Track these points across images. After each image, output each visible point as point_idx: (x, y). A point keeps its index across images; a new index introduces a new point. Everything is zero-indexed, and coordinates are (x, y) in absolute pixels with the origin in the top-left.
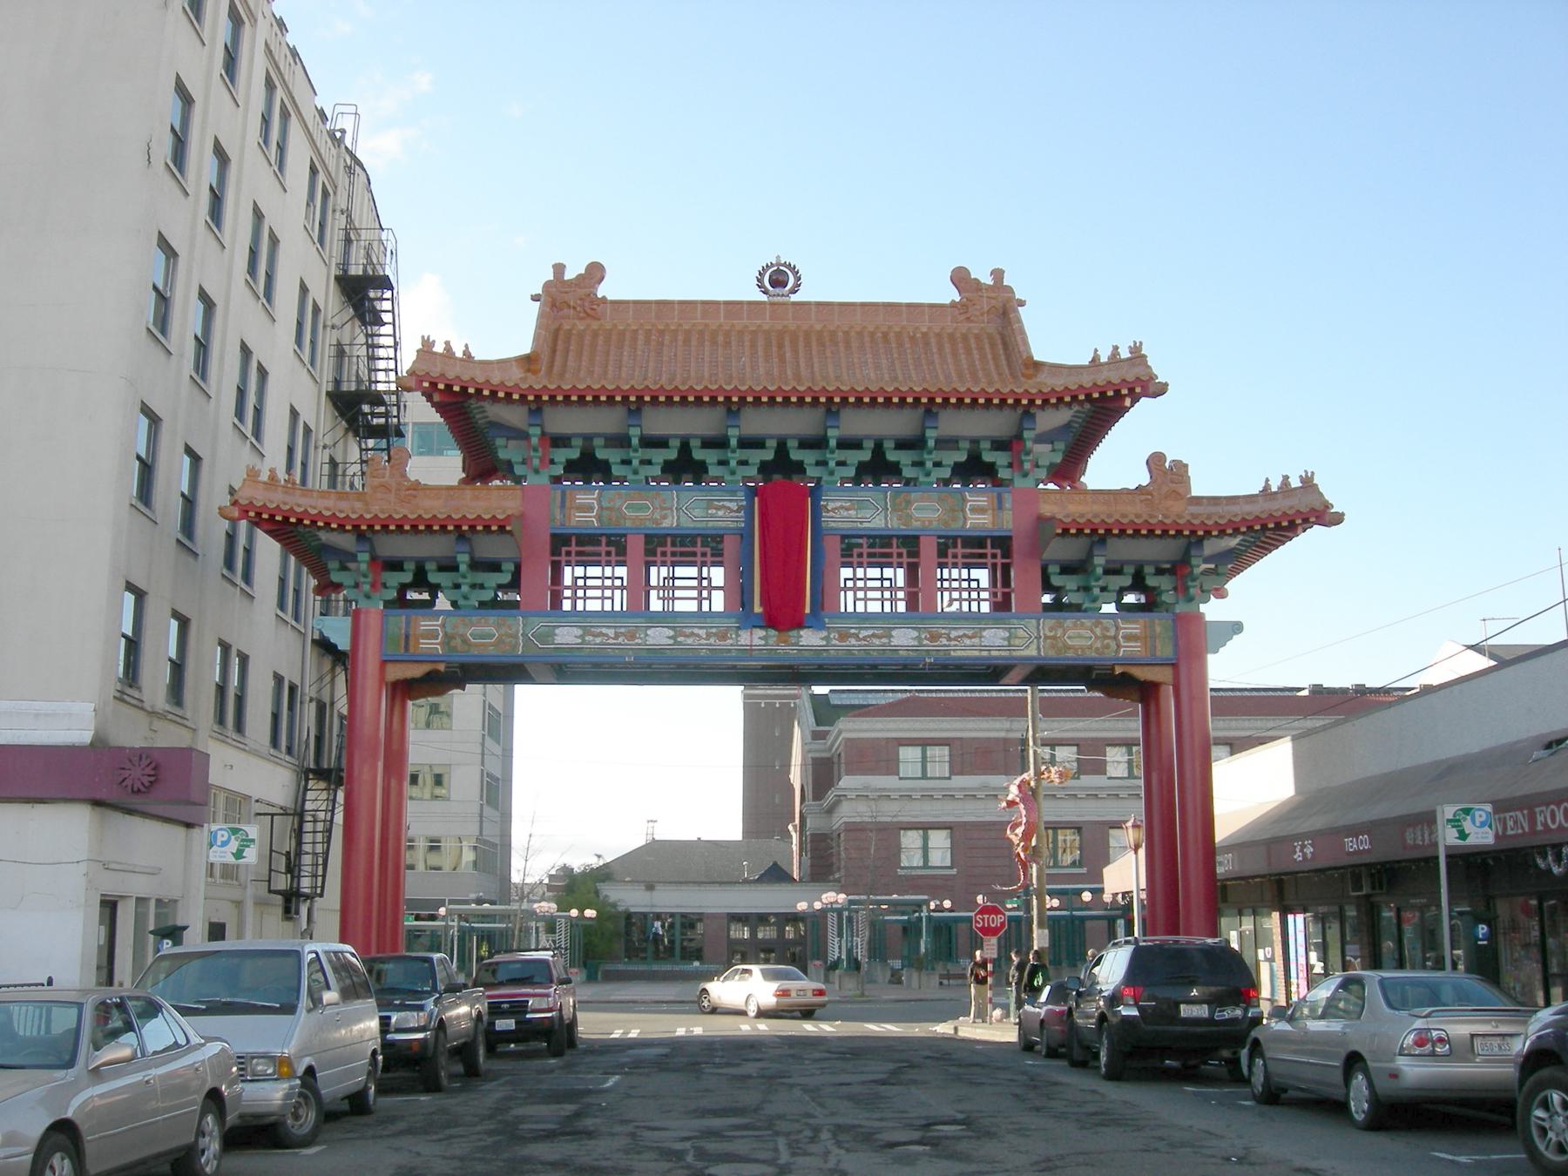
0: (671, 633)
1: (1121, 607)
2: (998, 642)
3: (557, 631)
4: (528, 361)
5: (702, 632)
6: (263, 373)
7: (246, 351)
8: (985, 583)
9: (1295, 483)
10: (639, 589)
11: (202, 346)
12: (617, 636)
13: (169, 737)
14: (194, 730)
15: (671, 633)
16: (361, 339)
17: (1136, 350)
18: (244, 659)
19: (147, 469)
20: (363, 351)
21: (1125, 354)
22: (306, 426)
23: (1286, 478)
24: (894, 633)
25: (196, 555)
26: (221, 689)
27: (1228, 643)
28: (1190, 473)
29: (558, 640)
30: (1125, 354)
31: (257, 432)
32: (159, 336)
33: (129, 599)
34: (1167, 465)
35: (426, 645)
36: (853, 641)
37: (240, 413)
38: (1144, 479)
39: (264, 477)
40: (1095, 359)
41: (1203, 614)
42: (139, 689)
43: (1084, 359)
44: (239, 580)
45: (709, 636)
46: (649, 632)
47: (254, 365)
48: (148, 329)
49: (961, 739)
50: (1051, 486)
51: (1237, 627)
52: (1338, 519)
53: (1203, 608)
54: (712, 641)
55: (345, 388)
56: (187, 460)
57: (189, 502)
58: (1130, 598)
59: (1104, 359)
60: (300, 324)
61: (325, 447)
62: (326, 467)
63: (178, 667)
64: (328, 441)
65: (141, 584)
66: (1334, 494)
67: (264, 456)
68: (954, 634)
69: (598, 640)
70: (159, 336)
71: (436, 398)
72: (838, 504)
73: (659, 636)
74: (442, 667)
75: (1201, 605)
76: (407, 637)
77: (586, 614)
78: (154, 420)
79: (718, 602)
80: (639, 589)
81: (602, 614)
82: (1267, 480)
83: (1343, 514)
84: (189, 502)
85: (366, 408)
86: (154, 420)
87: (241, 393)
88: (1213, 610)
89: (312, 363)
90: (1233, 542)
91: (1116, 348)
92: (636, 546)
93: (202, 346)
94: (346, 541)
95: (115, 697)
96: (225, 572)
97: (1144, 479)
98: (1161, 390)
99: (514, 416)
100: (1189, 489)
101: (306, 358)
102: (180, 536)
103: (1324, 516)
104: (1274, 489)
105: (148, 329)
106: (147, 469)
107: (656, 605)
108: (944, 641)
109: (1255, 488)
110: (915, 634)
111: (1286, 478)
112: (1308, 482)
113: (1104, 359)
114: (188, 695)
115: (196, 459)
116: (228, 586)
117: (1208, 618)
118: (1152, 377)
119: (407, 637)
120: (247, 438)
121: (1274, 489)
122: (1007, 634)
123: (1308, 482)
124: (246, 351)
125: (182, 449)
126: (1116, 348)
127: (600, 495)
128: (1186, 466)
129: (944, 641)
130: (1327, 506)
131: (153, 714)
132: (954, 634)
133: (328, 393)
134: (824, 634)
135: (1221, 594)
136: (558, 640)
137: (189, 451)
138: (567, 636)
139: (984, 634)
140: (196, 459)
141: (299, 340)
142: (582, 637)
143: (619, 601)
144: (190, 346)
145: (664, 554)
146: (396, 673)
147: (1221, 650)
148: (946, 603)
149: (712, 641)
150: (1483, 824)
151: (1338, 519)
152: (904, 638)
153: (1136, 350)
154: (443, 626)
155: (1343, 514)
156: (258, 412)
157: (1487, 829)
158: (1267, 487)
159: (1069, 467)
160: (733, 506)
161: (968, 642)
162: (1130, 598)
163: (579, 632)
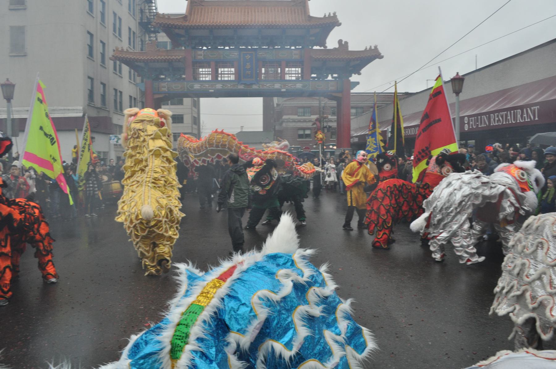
0: (221, 85)
1: (333, 77)
2: (300, 87)
3: (195, 85)
4: (184, 17)
5: (229, 85)
6: (120, 19)
7: (115, 14)
8: (300, 72)
9: (373, 48)
10: (215, 74)
11: (103, 14)
12: (209, 86)
13: (103, 114)
14: (109, 111)
15: (221, 85)
16: (147, 8)
17: (334, 14)
18: (121, 92)
19: (91, 48)
20: (147, 11)
21: (332, 15)
22: (134, 33)
23: (371, 46)
24: (275, 85)
25: (105, 68)
26: (115, 101)
27: (356, 87)
28: (349, 45)
29: (195, 88)
30: (332, 15)
31: (120, 34)
32: (90, 13)
33: (90, 80)
34: (343, 43)
35: (163, 89)
36: (265, 87)
37: (115, 30)
38: (337, 46)
39: (120, 49)
40: (325, 15)
42: (94, 102)
43: (322, 16)
44: (118, 73)
45: (231, 86)
46: (217, 85)
47: (117, 17)
48: (87, 12)
50: (317, 48)
51: (358, 83)
53: (350, 78)
54: (232, 87)
55: (144, 21)
56: (101, 44)
57: (103, 55)
58: (335, 75)
59: (327, 16)
60: (129, 5)
61: (139, 37)
62: (140, 43)
63: (103, 97)
64: (140, 35)
65: (92, 76)
67: (121, 41)
68: (289, 85)
69: (204, 87)
70: (90, 13)
71: (161, 28)
72: (261, 53)
73: (219, 86)
74: (167, 95)
75: (350, 78)
76: (158, 88)
77: (203, 81)
78: (91, 35)
79: (232, 78)
80: (215, 74)
81: (206, 81)
84: (103, 55)
85: (150, 26)
86: (91, 35)
87: (115, 25)
88: (354, 78)
89: (134, 14)
91: (330, 13)
92: (213, 64)
93: (103, 14)
94: (142, 64)
95: (88, 105)
96: (114, 71)
97: (337, 46)
98: (339, 25)
99: (182, 32)
101: (132, 14)
102: (101, 64)
103: (380, 57)
104: (368, 49)
105: (87, 12)
106: (91, 48)
107: (219, 79)
108: (287, 87)
109: (363, 49)
110: (280, 85)
111: (371, 46)
112: (376, 47)
113: (327, 16)
114: (107, 103)
115: (104, 44)
116: (115, 75)
118: (338, 21)
119: (158, 88)
120: (116, 37)
122: (302, 85)
123: (376, 47)
124: (115, 14)
125: (99, 42)
126: (330, 13)
127: (203, 53)
129: (287, 87)
130: (380, 54)
131: (97, 108)
132: (289, 85)
133: (139, 23)
134: (258, 85)
135: (359, 74)
136: (195, 88)
137: (101, 42)
138: (197, 86)
139: (297, 85)
140: (104, 44)
141: (130, 9)
142: (200, 87)
143: (209, 78)
144: (99, 15)
145: (220, 66)
146: (156, 96)
147: (354, 89)
148: (287, 77)
149: (232, 87)
152: (277, 86)
153: (334, 14)
154: (167, 85)
156: (120, 29)
158: (366, 49)
159: (322, 43)
160: (236, 54)
161: (292, 87)
162: (335, 75)
163: (199, 85)
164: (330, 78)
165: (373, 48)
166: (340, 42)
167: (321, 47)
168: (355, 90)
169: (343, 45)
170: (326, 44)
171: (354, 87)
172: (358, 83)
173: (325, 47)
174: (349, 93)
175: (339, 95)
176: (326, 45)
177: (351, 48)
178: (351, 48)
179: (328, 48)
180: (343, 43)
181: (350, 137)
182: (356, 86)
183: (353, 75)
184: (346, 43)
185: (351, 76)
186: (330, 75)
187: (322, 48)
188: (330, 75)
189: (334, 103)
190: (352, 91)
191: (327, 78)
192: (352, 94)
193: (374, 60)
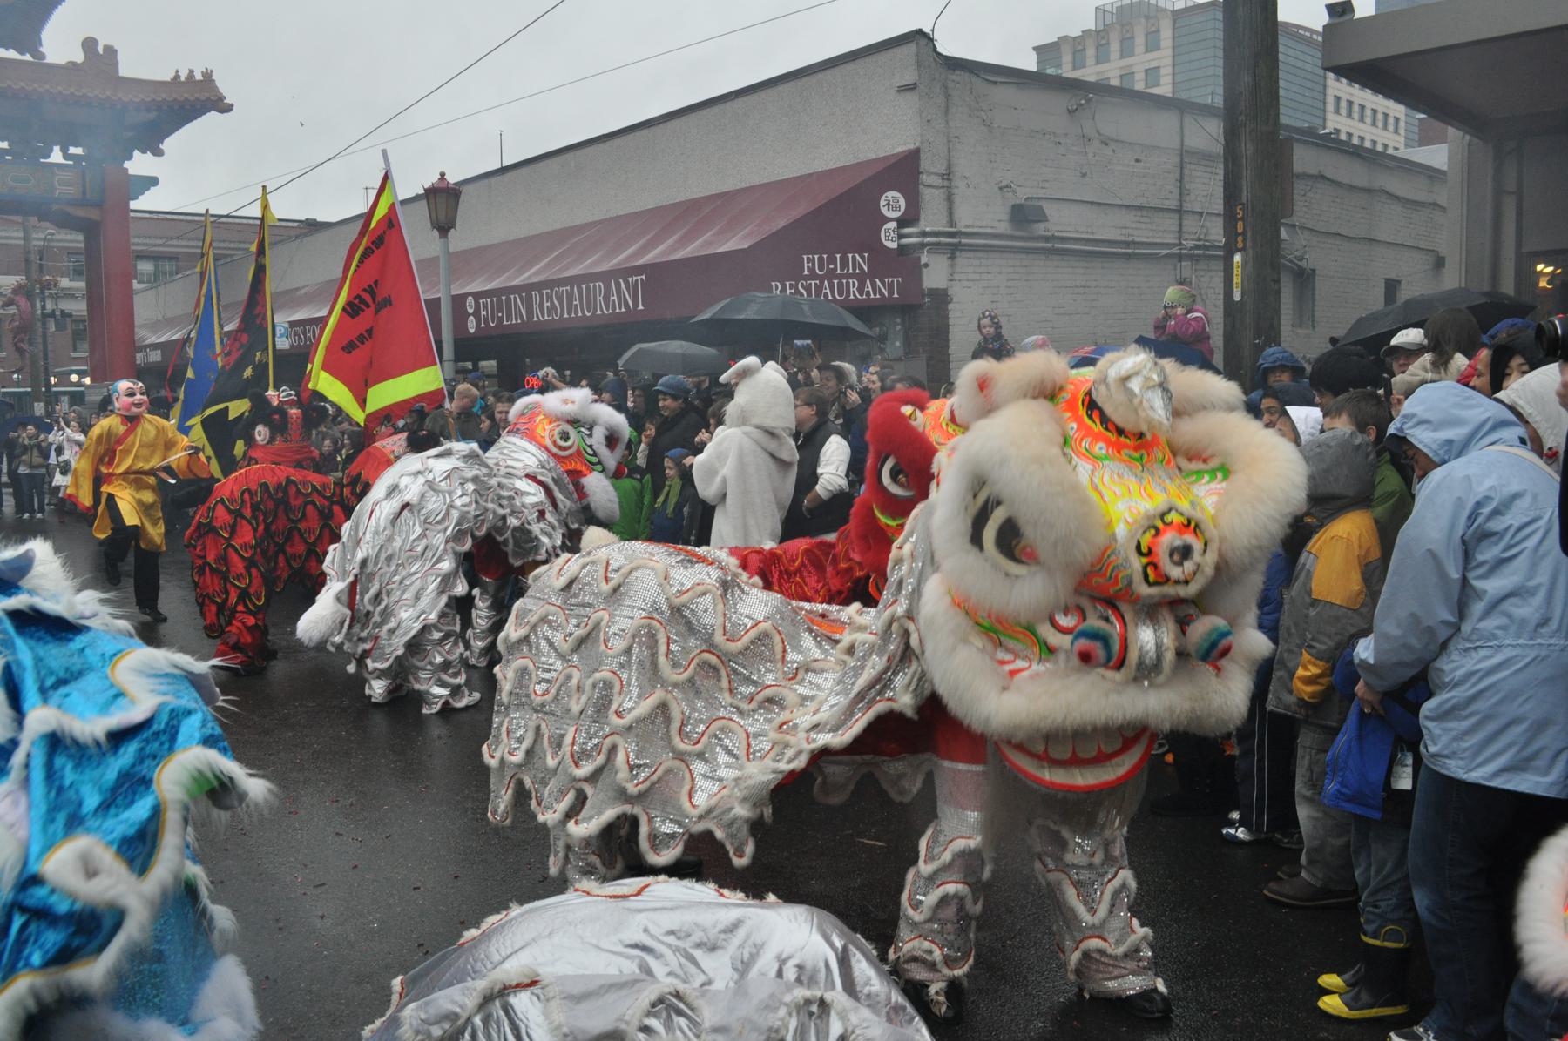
1: (66, 156)
9: (199, 77)
23: (191, 72)
28: (120, 57)
34: (100, 49)
38: (79, 57)
41: (127, 170)
49: (7, 245)
51: (153, 181)
52: (228, 108)
53: (127, 164)
58: (73, 150)
66: (226, 87)
75: (127, 164)
82: (177, 71)
83: (232, 105)
88: (139, 164)
90: (152, 115)
97: (79, 57)
100: (117, 71)
104: (183, 79)
111: (191, 72)
112: (208, 76)
117: (131, 172)
121: (183, 79)
128: (115, 52)
130: (222, 98)
135: (158, 153)
150: (281, 336)
151: (228, 108)
155: (232, 105)
157: (285, 339)
158: (177, 76)
159: (28, 39)
162: (73, 150)
164: (56, 156)
165: (199, 77)
166: (89, 44)
167: (22, 53)
168: (144, 203)
169: (100, 58)
170: (41, 45)
171: (143, 194)
172: (153, 181)
173: (43, 56)
174: (127, 209)
175: (94, 214)
176: (41, 49)
177: (124, 71)
178: (124, 71)
179: (48, 60)
180: (100, 49)
181: (133, 346)
182: (149, 189)
183: (136, 153)
184: (111, 51)
185: (130, 158)
186: (57, 149)
187: (28, 57)
188: (57, 149)
189: (76, 240)
190: (133, 205)
191: (48, 156)
192: (132, 214)
193: (205, 114)
